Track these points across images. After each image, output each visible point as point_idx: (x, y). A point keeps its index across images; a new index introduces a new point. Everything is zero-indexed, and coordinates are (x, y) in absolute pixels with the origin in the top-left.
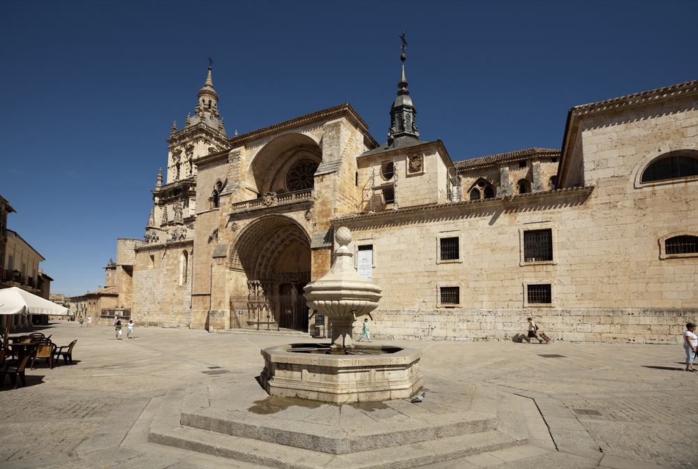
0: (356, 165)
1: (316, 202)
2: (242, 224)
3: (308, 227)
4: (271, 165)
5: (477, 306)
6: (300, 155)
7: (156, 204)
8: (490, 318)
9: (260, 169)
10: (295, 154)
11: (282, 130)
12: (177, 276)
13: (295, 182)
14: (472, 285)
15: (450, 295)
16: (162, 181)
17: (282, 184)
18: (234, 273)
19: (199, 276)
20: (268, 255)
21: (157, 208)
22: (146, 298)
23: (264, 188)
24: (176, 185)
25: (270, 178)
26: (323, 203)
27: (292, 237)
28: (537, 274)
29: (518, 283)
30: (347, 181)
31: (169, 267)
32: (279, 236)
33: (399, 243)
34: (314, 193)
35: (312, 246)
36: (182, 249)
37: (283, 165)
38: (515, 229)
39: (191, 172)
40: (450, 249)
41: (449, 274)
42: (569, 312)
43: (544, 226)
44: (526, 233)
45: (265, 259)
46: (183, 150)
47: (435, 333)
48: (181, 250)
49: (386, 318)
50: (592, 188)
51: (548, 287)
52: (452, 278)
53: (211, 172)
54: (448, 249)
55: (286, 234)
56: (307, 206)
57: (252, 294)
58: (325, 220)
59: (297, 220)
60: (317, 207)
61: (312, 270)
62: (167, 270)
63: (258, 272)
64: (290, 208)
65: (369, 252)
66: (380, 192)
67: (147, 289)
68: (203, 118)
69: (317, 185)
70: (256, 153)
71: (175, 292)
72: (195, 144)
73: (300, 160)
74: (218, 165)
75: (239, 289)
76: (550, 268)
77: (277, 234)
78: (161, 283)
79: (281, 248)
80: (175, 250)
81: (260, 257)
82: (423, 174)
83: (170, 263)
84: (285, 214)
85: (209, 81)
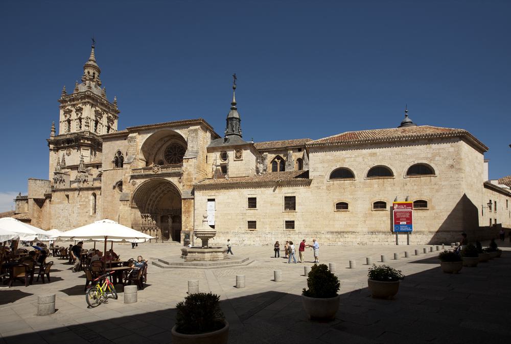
0: (206, 152)
1: (184, 173)
2: (139, 182)
3: (180, 187)
4: (154, 145)
5: (264, 230)
6: (173, 141)
7: (51, 150)
8: (269, 236)
9: (147, 149)
10: (169, 140)
11: (164, 127)
12: (88, 209)
13: (170, 156)
14: (262, 220)
15: (252, 225)
16: (55, 132)
17: (161, 157)
18: (134, 210)
19: (106, 210)
20: (154, 199)
21: (52, 153)
22: (63, 223)
23: (150, 158)
24: (68, 137)
25: (153, 152)
26: (188, 174)
27: (169, 189)
28: (289, 216)
29: (281, 219)
30: (202, 162)
31: (81, 203)
32: (160, 188)
33: (228, 199)
34: (183, 168)
35: (182, 197)
36: (92, 192)
37: (162, 146)
38: (281, 195)
39: (80, 127)
40: (252, 202)
41: (252, 215)
42: (301, 233)
43: (293, 195)
44: (285, 197)
45: (152, 201)
46: (74, 110)
47: (245, 243)
48: (91, 192)
49: (222, 235)
50: (311, 180)
51: (293, 222)
52: (253, 217)
53: (112, 144)
54: (252, 203)
55: (165, 187)
56: (179, 175)
57: (144, 222)
58: (189, 183)
59: (173, 182)
60: (185, 176)
61: (182, 210)
62: (80, 205)
63: (148, 209)
64: (170, 175)
65: (213, 202)
66: (219, 168)
67: (64, 217)
68: (90, 87)
69: (185, 164)
70: (146, 138)
71: (87, 219)
72: (83, 107)
73: (173, 144)
74: (117, 140)
75: (137, 219)
76: (294, 213)
77: (160, 187)
78: (75, 213)
79: (162, 195)
80: (85, 192)
81: (149, 200)
82: (242, 160)
83: (82, 200)
84: (166, 178)
85: (92, 57)
